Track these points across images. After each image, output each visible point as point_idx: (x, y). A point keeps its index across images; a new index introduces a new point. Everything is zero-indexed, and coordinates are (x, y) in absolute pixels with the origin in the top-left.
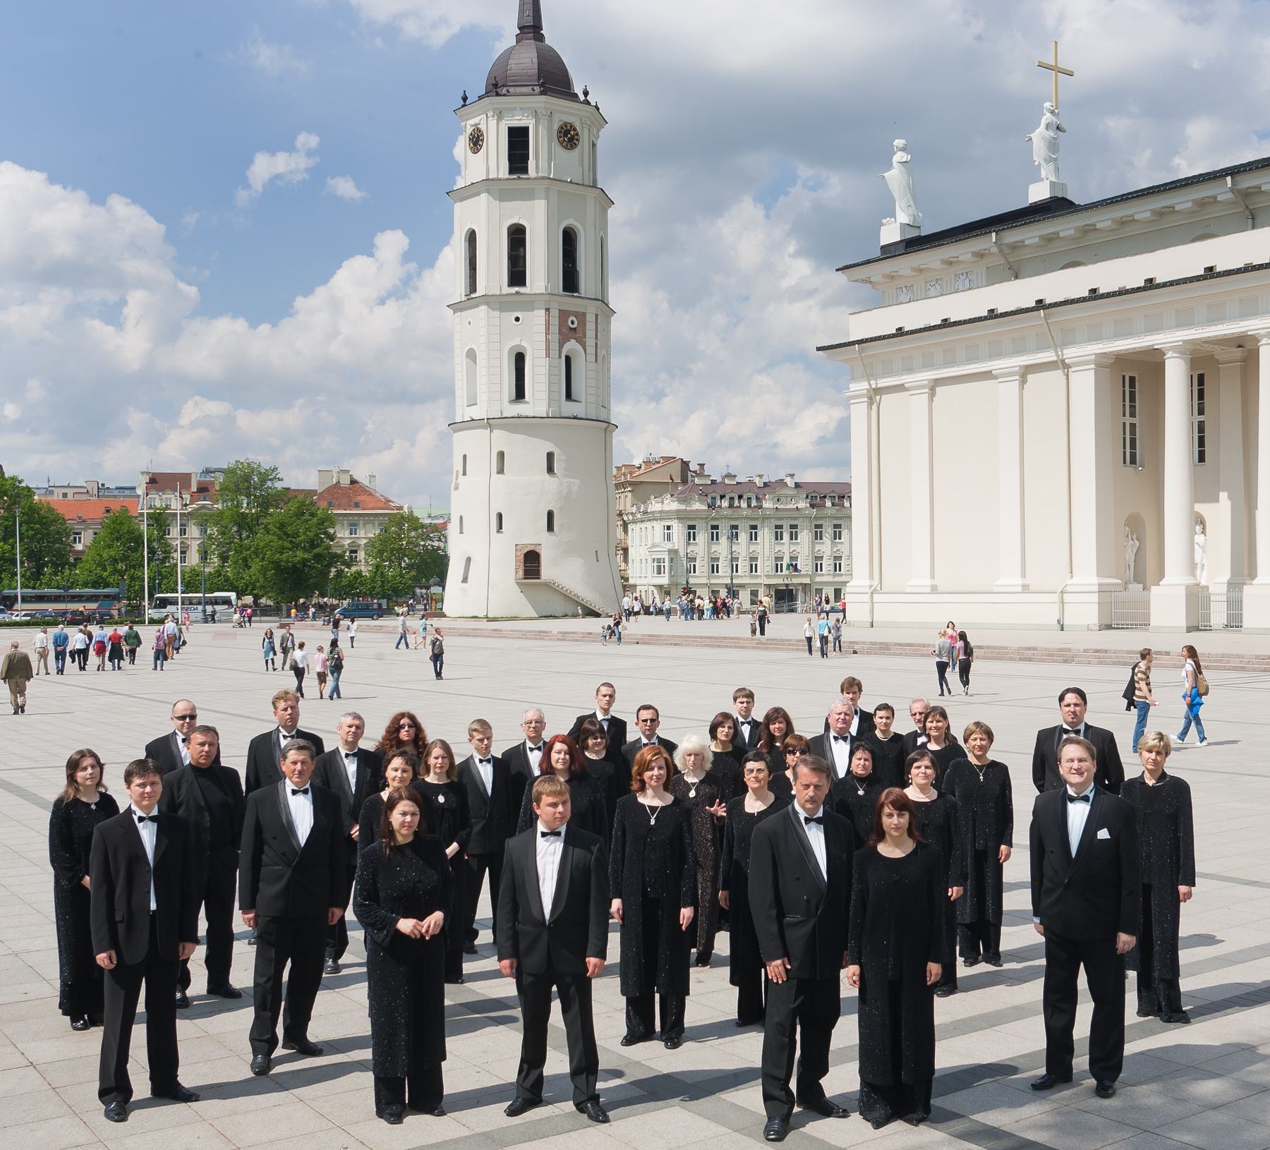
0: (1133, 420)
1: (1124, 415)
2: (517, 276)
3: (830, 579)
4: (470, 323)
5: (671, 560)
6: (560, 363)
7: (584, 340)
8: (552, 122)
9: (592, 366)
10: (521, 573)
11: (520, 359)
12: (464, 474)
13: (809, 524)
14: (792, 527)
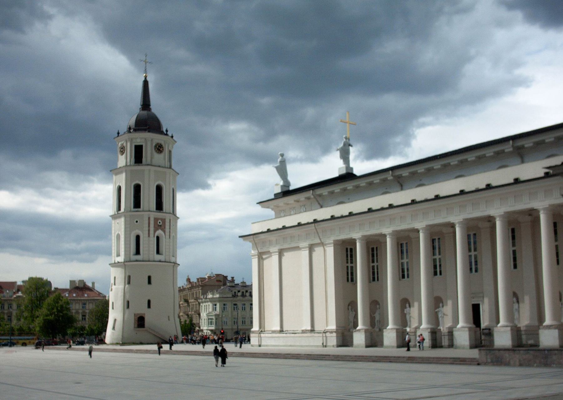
0: (352, 265)
1: (347, 263)
2: (137, 204)
5: (216, 319)
6: (154, 239)
10: (136, 326)
11: (138, 238)
12: (115, 284)
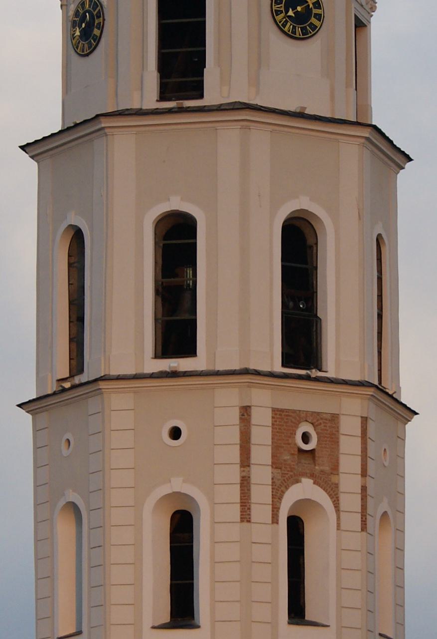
7: (334, 479)
9: (355, 540)
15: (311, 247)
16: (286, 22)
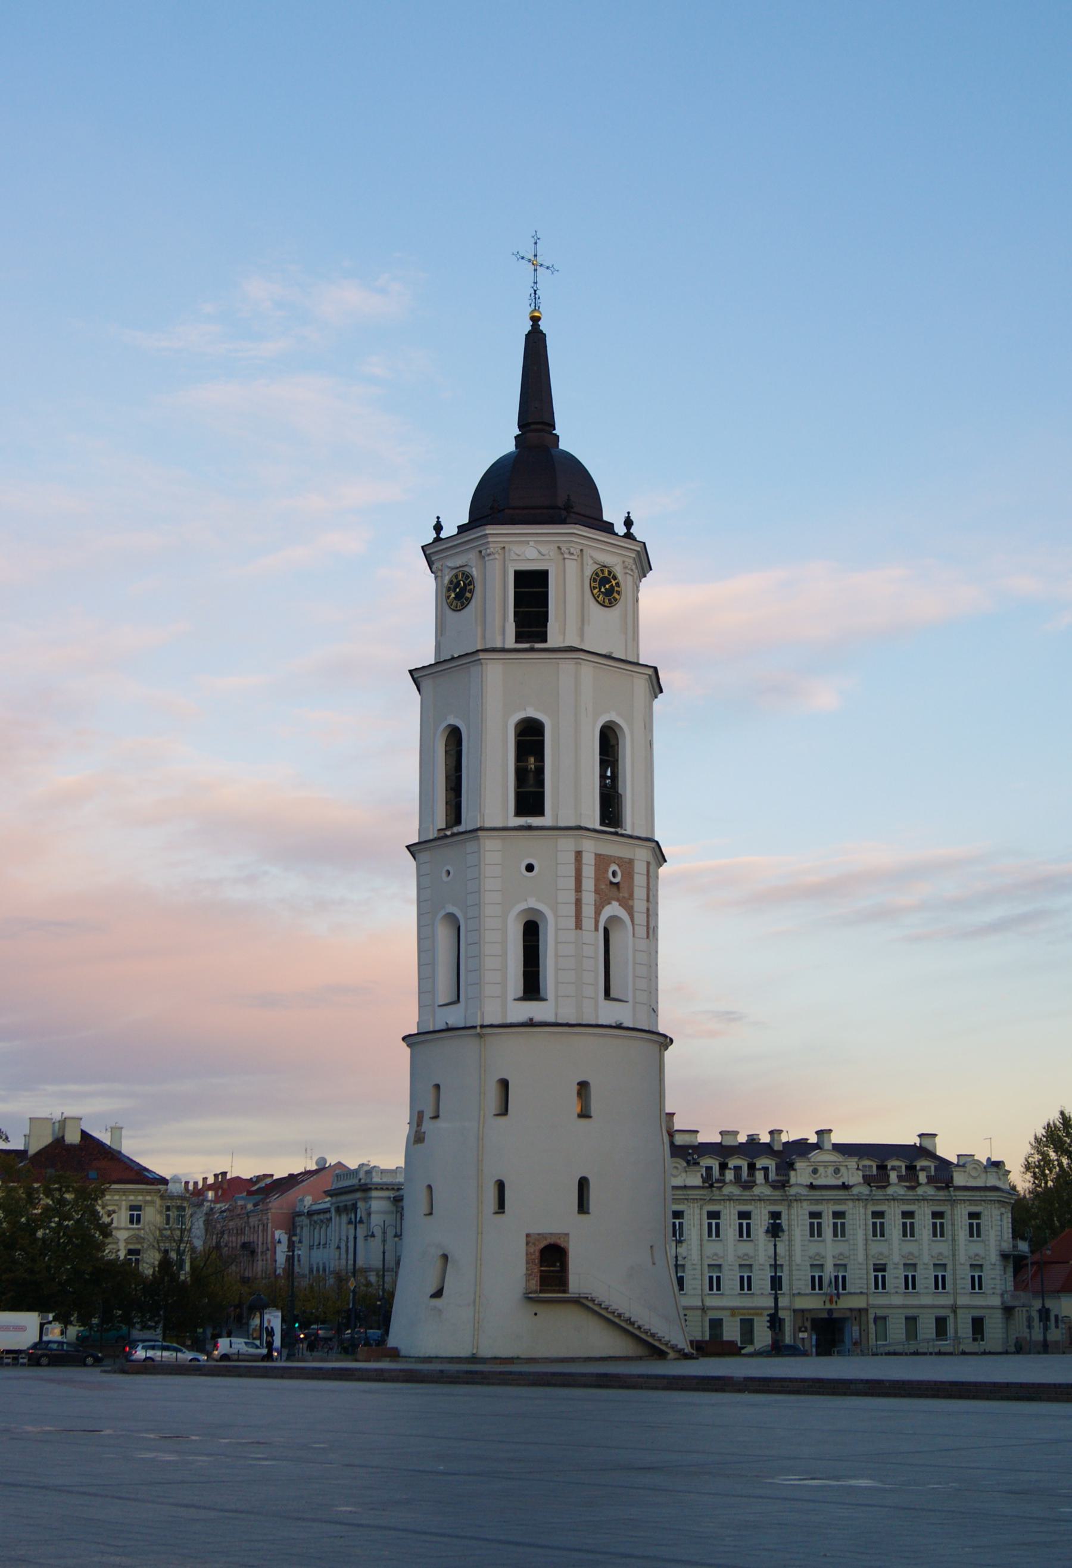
3: (897, 1300)
4: (448, 873)
7: (630, 902)
8: (582, 564)
10: (535, 1284)
11: (532, 931)
13: (862, 1211)
14: (838, 1215)
15: (613, 746)
16: (599, 594)
